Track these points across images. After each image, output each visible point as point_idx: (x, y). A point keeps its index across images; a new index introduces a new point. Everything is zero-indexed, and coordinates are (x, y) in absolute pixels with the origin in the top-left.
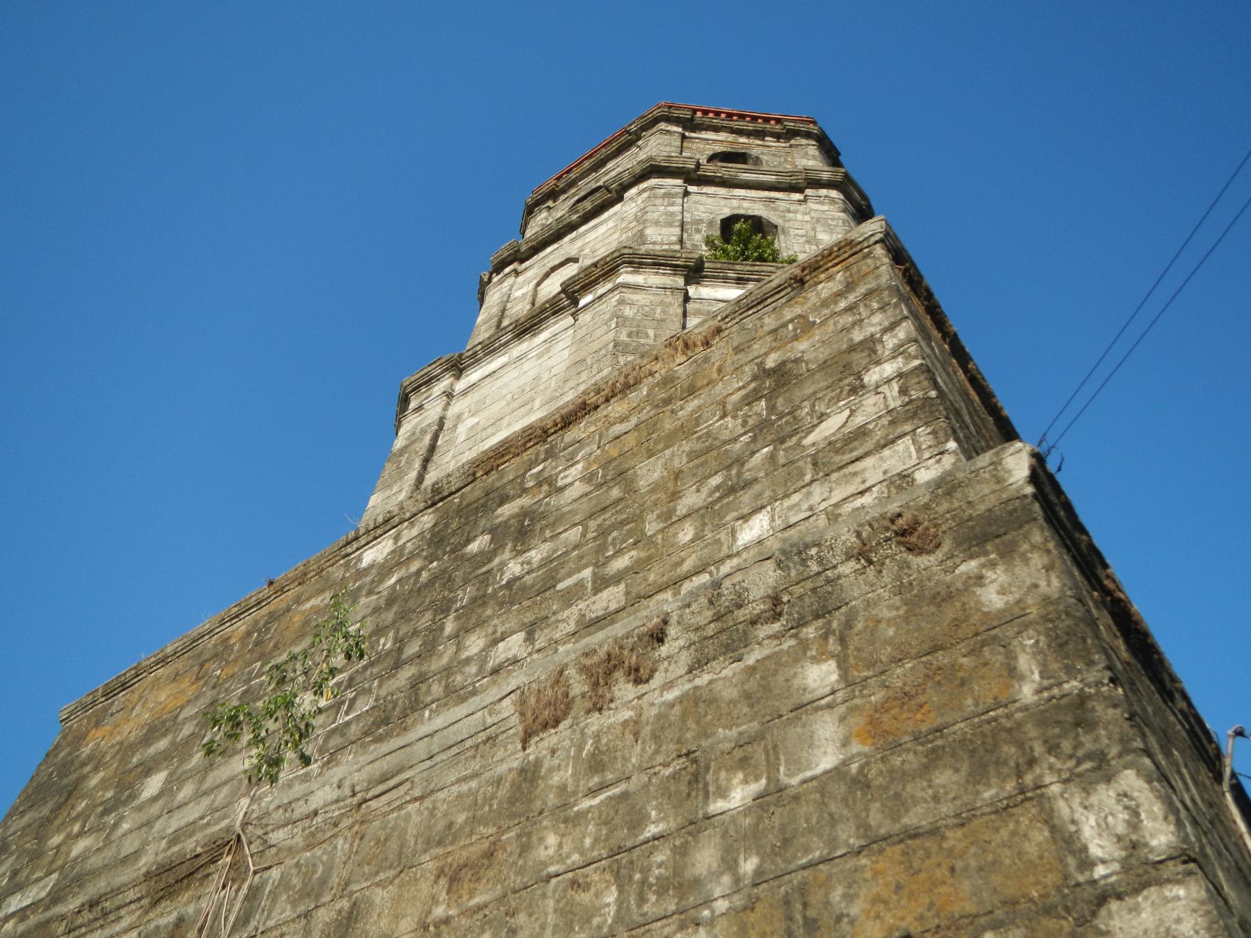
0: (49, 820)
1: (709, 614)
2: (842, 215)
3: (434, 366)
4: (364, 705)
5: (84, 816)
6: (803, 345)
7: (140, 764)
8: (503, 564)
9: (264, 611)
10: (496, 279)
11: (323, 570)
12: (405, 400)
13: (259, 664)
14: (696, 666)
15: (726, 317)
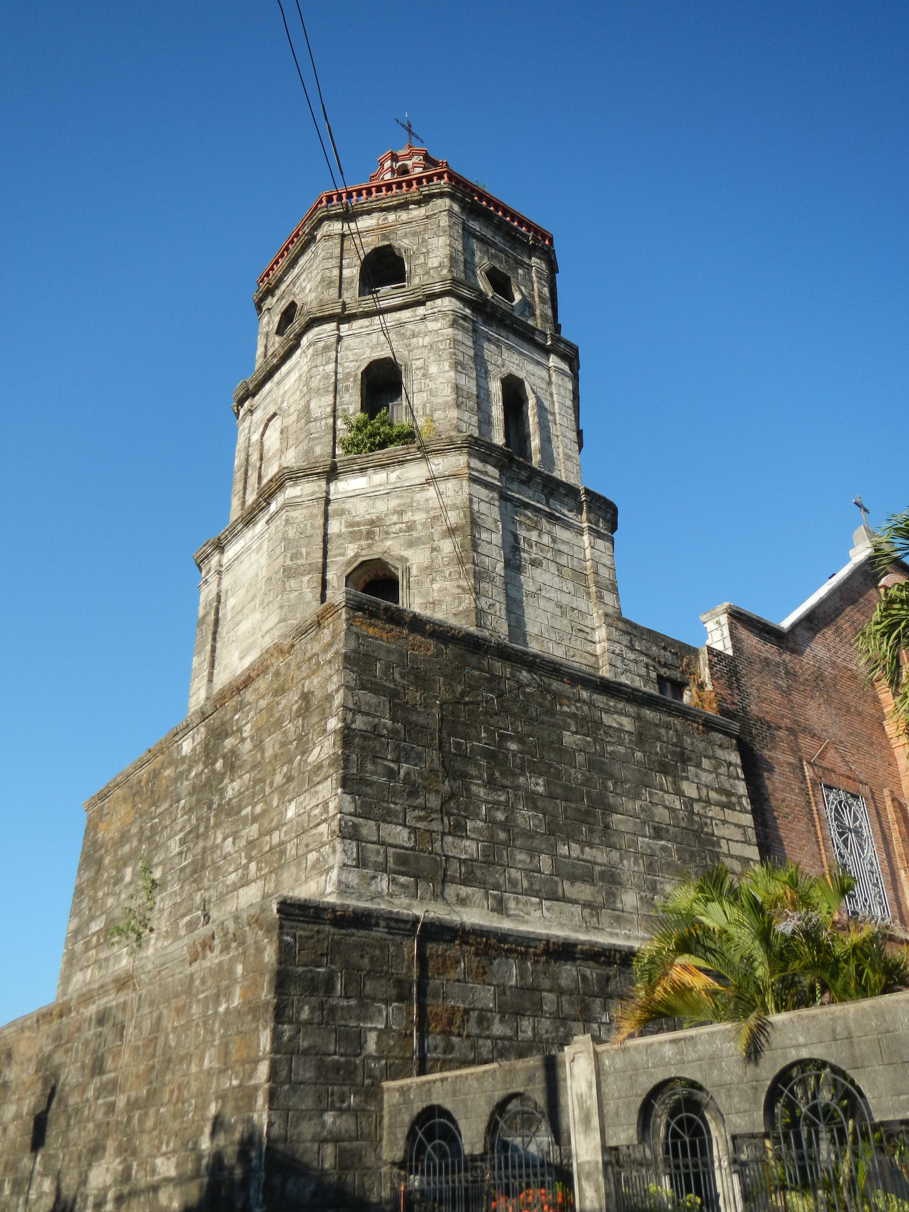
0: (95, 880)
2: (450, 330)
5: (106, 883)
6: (316, 681)
7: (122, 858)
8: (227, 785)
13: (153, 808)
14: (222, 951)
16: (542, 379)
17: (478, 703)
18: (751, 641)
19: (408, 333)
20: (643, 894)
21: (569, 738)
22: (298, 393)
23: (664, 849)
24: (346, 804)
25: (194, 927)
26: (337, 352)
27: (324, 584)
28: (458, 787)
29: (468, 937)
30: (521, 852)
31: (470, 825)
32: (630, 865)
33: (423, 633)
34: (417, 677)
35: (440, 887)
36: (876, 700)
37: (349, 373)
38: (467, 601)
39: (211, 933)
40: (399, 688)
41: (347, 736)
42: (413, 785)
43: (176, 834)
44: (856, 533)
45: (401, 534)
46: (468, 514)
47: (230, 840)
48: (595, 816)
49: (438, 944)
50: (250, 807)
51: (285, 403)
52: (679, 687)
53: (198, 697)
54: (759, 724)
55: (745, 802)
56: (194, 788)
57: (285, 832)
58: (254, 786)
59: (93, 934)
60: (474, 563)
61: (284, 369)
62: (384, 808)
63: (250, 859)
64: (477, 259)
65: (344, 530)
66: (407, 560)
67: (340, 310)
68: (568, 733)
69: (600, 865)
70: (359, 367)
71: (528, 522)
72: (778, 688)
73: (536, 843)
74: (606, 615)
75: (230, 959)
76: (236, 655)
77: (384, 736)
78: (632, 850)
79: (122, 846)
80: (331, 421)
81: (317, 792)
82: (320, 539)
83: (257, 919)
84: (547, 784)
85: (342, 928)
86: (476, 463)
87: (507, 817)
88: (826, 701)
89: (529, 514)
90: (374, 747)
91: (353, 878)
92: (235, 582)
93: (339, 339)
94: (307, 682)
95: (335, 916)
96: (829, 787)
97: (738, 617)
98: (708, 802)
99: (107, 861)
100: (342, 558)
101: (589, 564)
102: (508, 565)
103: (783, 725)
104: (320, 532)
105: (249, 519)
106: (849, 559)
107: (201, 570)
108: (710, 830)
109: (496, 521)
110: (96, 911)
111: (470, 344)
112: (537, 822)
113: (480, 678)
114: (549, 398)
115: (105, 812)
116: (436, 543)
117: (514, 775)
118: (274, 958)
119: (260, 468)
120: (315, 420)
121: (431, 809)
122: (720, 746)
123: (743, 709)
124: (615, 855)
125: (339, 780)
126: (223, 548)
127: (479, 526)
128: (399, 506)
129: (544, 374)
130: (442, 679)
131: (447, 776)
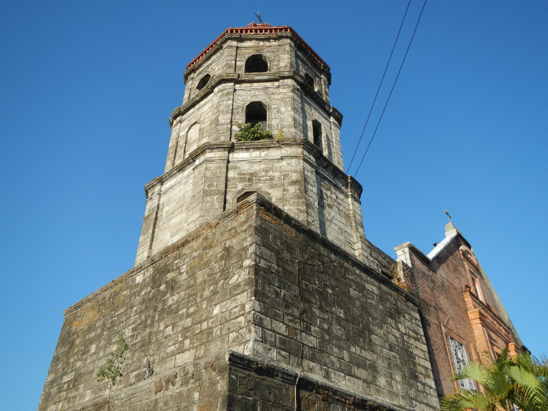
0: (68, 353)
1: (183, 374)
2: (291, 93)
3: (154, 181)
4: (139, 338)
6: (234, 241)
8: (168, 298)
9: (113, 290)
10: (175, 122)
11: (126, 280)
12: (147, 192)
13: (114, 312)
14: (182, 385)
15: (220, 219)
17: (314, 266)
18: (418, 262)
19: (270, 92)
20: (387, 379)
21: (353, 293)
22: (211, 113)
23: (394, 356)
24: (257, 306)
25: (141, 377)
26: (233, 96)
27: (225, 201)
28: (307, 307)
29: (319, 389)
30: (335, 348)
31: (313, 328)
32: (381, 363)
33: (290, 224)
34: (287, 246)
35: (300, 359)
36: (464, 301)
37: (240, 106)
38: (302, 217)
39: (175, 373)
40: (280, 250)
41: (257, 269)
42: (287, 302)
43: (129, 325)
44: (447, 225)
45: (267, 181)
46: (303, 175)
47: (170, 327)
48: (365, 334)
49: (305, 391)
50: (185, 309)
51: (202, 118)
52: (391, 278)
53: (142, 256)
54: (423, 302)
55: (423, 338)
56: (144, 301)
57: (212, 322)
58: (189, 297)
59: (65, 383)
60: (306, 199)
61: (202, 103)
62: (274, 312)
63: (185, 338)
64: (300, 68)
65: (236, 176)
66: (270, 194)
67: (237, 77)
68: (352, 289)
69: (369, 360)
70: (244, 104)
71: (326, 186)
72: (429, 287)
73: (341, 343)
74: (361, 237)
75: (188, 390)
76: (168, 235)
77: (273, 273)
78: (381, 355)
79: (90, 333)
80: (229, 126)
81: (236, 300)
82: (224, 179)
83: (213, 365)
84: (345, 314)
85: (260, 375)
86: (306, 153)
87: (328, 327)
88: (446, 297)
89: (327, 183)
90: (269, 278)
91: (260, 348)
92: (169, 199)
93: (235, 90)
94: (228, 242)
95: (258, 367)
96: (452, 339)
97: (413, 250)
99: (78, 342)
100: (235, 189)
101: (351, 212)
103: (432, 305)
104: (224, 175)
105: (181, 168)
106: (445, 237)
107: (147, 195)
108: (411, 351)
109: (314, 182)
110: (68, 370)
112: (341, 333)
113: (315, 253)
114: (330, 135)
115: (78, 315)
116: (286, 187)
117: (331, 306)
118: (226, 388)
119: (185, 147)
120: (221, 125)
121: (295, 316)
122: (412, 309)
123: (417, 293)
124: (375, 356)
125: (253, 293)
126: (163, 183)
128: (266, 168)
129: (328, 124)
130: (298, 250)
131: (302, 301)
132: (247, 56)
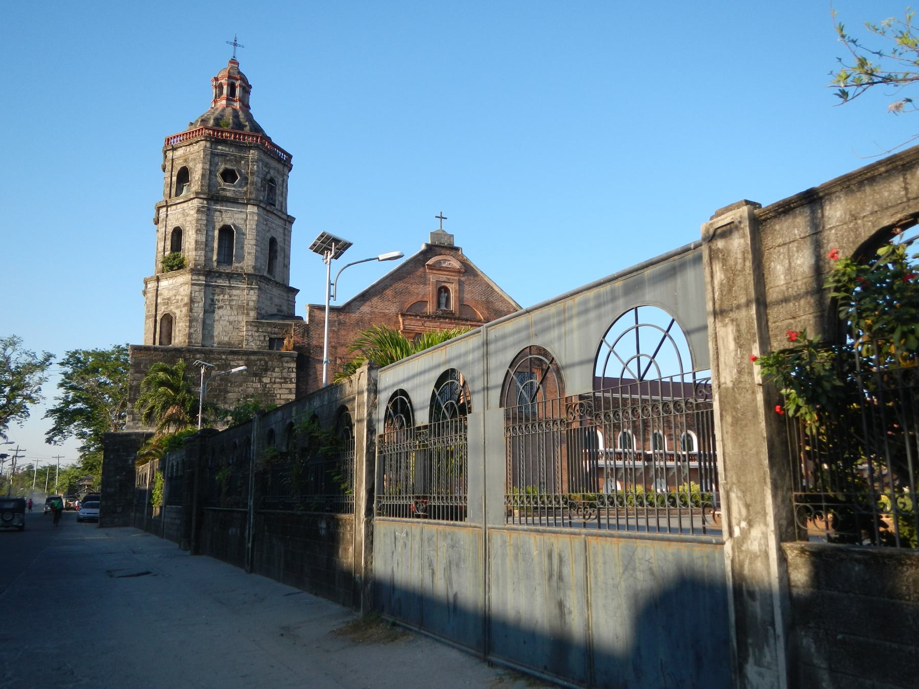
16: (243, 219)
27: (156, 321)
36: (398, 322)
60: (190, 317)
86: (195, 277)
91: (131, 424)
93: (167, 216)
98: (275, 383)
102: (205, 312)
104: (155, 303)
109: (202, 299)
111: (204, 218)
122: (287, 362)
123: (308, 344)
127: (194, 302)
132: (179, 168)
